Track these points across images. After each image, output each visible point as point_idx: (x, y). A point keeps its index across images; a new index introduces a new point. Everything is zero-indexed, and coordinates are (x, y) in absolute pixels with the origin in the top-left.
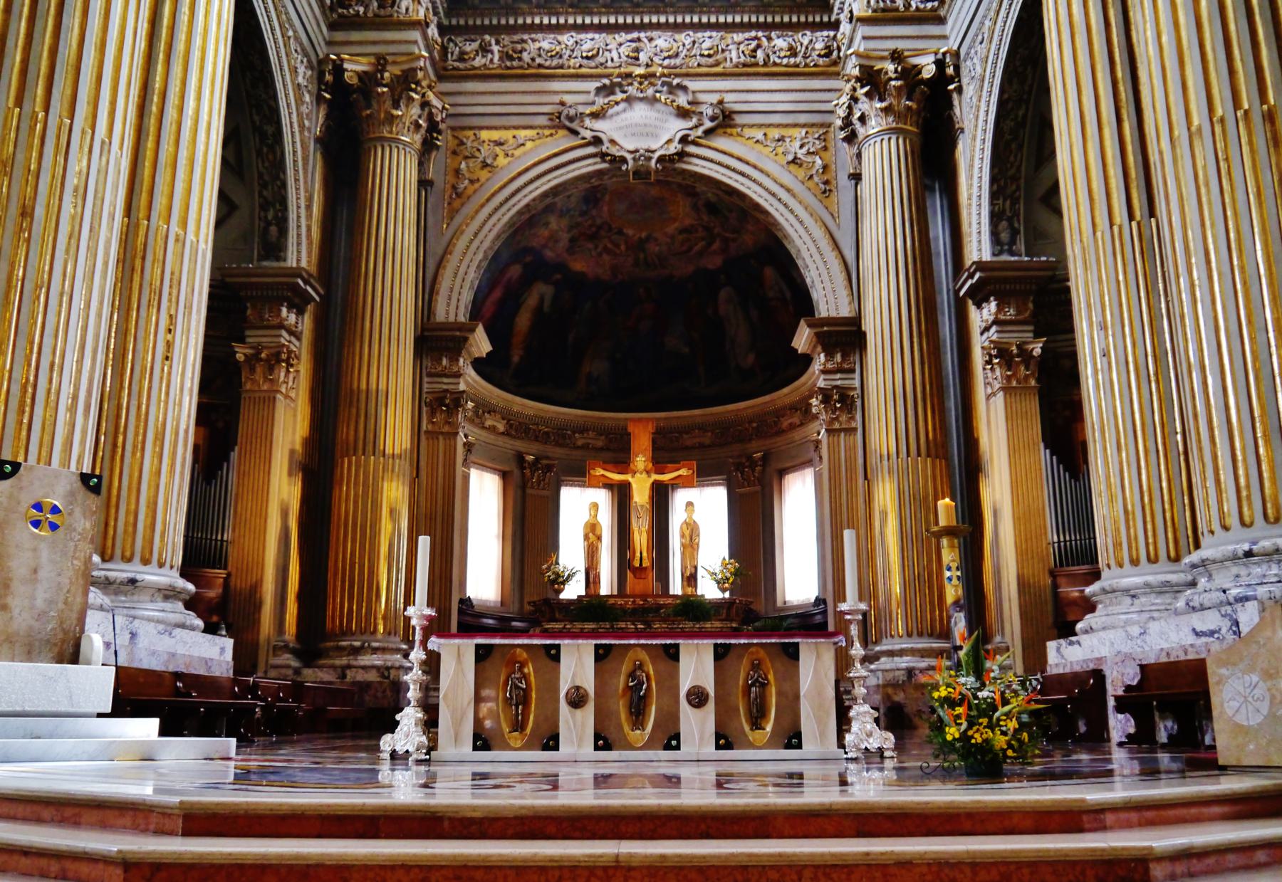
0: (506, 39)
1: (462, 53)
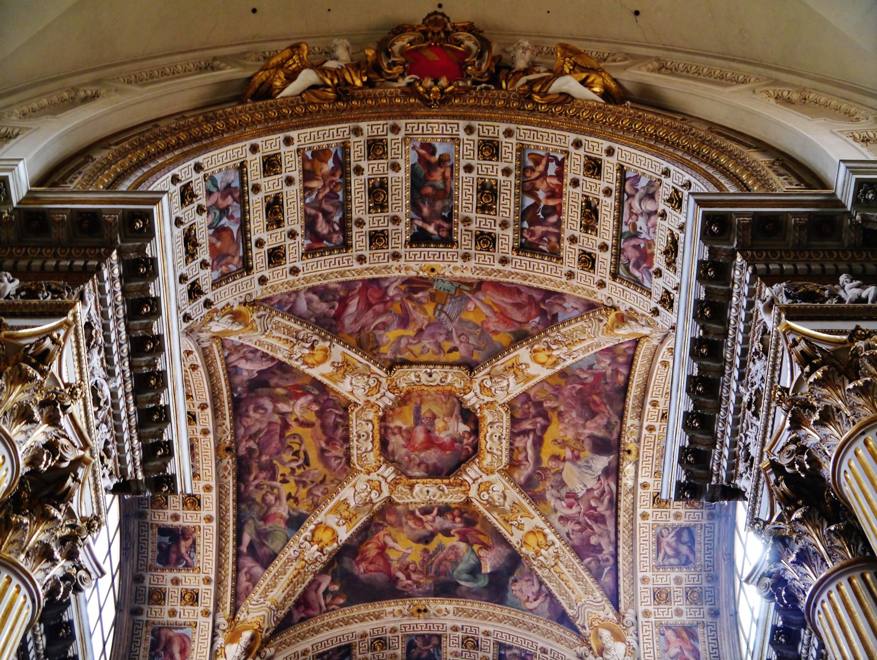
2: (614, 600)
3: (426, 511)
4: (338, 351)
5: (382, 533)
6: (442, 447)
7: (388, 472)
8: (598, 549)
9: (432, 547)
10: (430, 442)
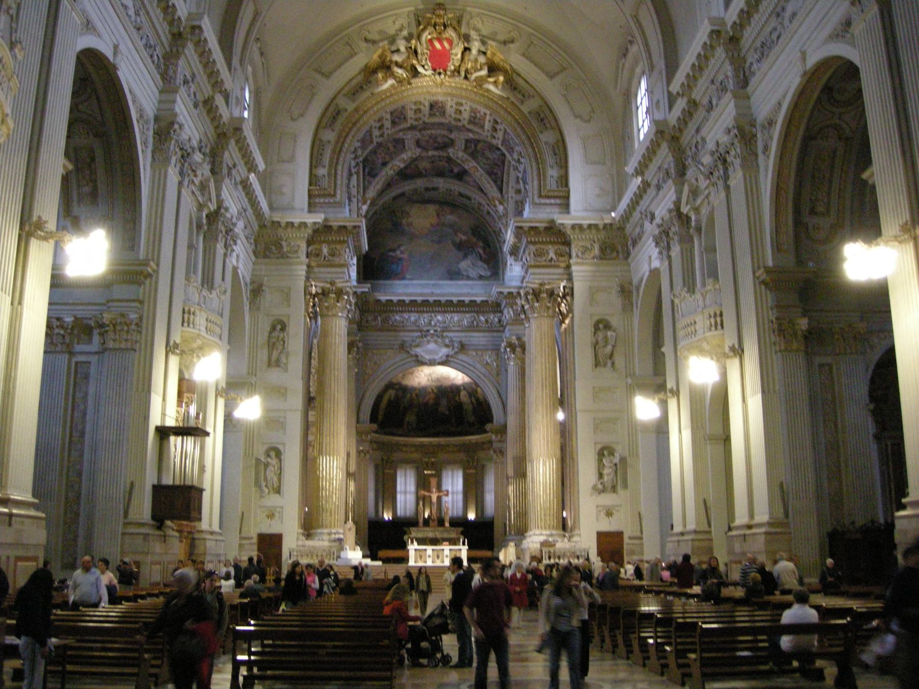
0: (384, 316)
2: (501, 190)
3: (433, 156)
4: (401, 134)
5: (416, 162)
6: (439, 143)
7: (419, 150)
8: (496, 174)
10: (435, 141)
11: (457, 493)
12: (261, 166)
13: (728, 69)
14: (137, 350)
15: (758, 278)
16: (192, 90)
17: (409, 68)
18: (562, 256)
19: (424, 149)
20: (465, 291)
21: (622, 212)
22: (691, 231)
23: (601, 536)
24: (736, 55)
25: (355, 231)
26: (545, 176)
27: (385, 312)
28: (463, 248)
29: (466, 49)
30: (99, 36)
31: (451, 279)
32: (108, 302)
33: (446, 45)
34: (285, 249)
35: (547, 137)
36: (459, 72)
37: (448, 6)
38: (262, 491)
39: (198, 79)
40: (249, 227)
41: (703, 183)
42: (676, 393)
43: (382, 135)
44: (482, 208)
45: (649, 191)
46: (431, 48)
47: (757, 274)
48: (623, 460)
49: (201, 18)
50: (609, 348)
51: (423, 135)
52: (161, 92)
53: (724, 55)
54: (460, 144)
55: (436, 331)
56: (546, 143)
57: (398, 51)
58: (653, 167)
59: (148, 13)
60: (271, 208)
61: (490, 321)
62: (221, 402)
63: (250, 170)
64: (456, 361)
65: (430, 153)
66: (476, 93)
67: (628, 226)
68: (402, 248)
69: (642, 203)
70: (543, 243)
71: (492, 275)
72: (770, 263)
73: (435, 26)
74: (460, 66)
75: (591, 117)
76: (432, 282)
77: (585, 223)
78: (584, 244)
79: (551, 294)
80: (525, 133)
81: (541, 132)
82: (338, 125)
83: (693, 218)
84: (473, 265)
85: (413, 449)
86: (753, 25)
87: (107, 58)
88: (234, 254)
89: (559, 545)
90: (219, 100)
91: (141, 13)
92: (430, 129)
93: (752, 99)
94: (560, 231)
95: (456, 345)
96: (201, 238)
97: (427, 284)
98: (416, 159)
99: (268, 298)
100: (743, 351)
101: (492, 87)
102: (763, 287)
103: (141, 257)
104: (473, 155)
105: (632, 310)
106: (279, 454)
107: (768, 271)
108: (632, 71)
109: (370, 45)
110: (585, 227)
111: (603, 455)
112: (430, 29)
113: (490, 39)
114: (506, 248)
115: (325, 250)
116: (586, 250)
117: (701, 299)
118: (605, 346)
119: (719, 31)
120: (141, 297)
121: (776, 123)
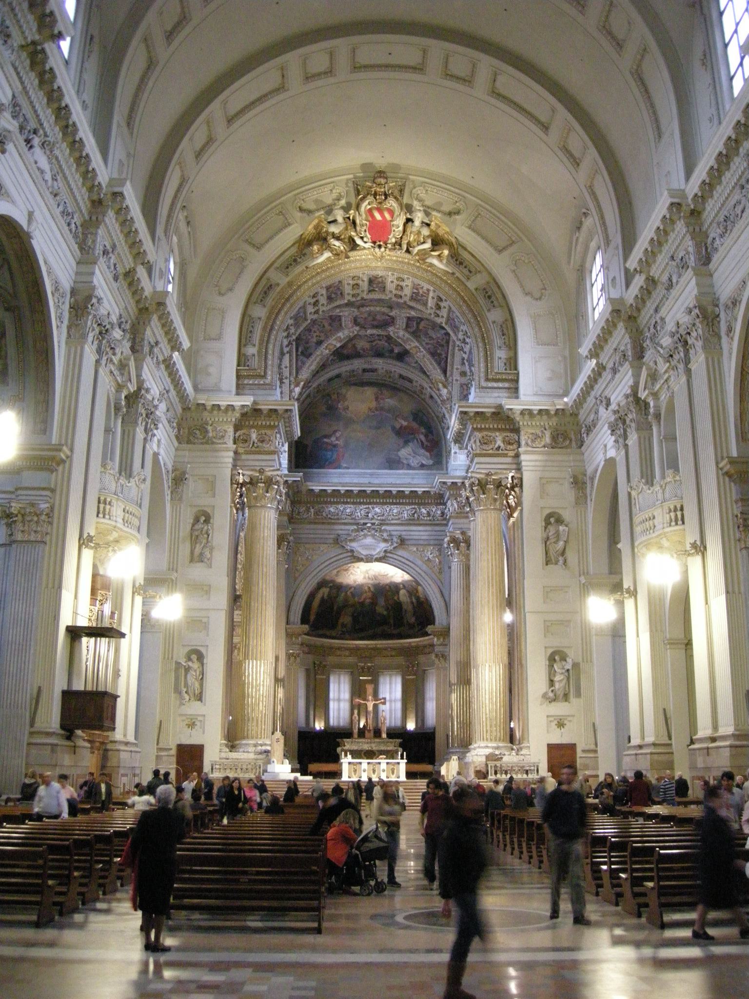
1: (299, 512)
2: (445, 372)
4: (338, 310)
5: (353, 342)
7: (357, 328)
8: (440, 355)
9: (374, 344)
10: (374, 320)
11: (395, 701)
12: (186, 344)
13: (689, 245)
14: (48, 542)
15: (721, 469)
16: (112, 261)
17: (346, 240)
18: (510, 444)
19: (363, 327)
20: (407, 480)
21: (575, 397)
22: (650, 417)
23: (552, 748)
24: (697, 229)
25: (286, 416)
26: (492, 359)
27: (319, 503)
28: (404, 435)
29: (409, 221)
30: (13, 202)
31: (391, 468)
32: (17, 489)
33: (387, 216)
34: (210, 435)
35: (495, 316)
36: (400, 245)
37: (389, 175)
38: (182, 698)
39: (119, 249)
40: (171, 409)
41: (662, 367)
42: (633, 593)
43: (317, 312)
44: (424, 391)
45: (604, 374)
46: (370, 219)
47: (721, 465)
48: (576, 665)
49: (123, 185)
50: (561, 544)
51: (362, 313)
52: (78, 263)
53: (684, 230)
54: (401, 323)
55: (373, 524)
56: (494, 322)
57: (334, 221)
58: (609, 349)
59: (66, 178)
60: (196, 388)
61: (432, 514)
62: (139, 599)
63: (173, 349)
64: (395, 557)
65: (369, 332)
66: (418, 267)
67: (582, 412)
68: (338, 434)
69: (596, 387)
70: (489, 429)
71: (434, 465)
72: (734, 454)
73: (375, 195)
74: (401, 238)
75: (542, 294)
76: (369, 471)
77: (536, 408)
78: (533, 431)
79: (499, 485)
80: (471, 311)
81: (489, 310)
82: (269, 301)
83: (652, 404)
84: (415, 453)
85: (347, 653)
86: (715, 198)
87: (21, 226)
88: (155, 439)
89: (506, 759)
90: (141, 272)
91: (59, 178)
92: (370, 306)
93: (716, 276)
94: (508, 417)
95: (395, 540)
96: (120, 421)
97: (366, 474)
98: (355, 336)
99: (192, 487)
100: (705, 548)
101: (435, 262)
102: (727, 479)
103: (53, 442)
104: (416, 334)
105: (586, 502)
106: (200, 657)
107: (732, 461)
108: (587, 248)
109: (305, 215)
110: (535, 412)
111: (555, 660)
112: (370, 198)
113: (434, 210)
114: (450, 435)
115: (254, 436)
116: (536, 437)
117: (661, 491)
118: (556, 542)
119: (679, 204)
120: (52, 486)
121: (740, 302)
